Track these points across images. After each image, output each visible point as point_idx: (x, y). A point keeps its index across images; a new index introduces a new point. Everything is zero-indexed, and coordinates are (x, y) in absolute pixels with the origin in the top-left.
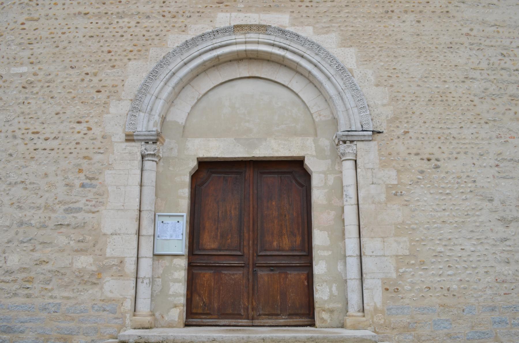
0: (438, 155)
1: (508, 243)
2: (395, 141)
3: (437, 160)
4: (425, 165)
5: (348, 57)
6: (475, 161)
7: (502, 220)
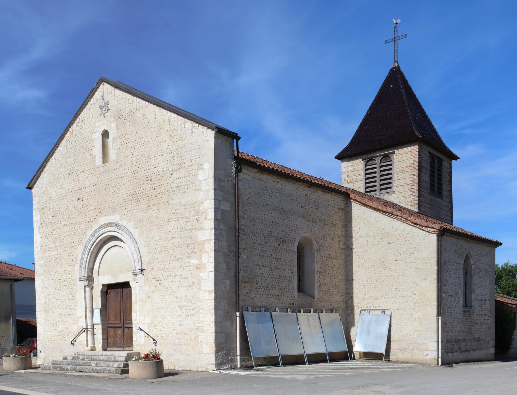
0: (161, 278)
1: (181, 317)
2: (150, 272)
3: (161, 281)
4: (157, 283)
6: (173, 280)
7: (180, 306)
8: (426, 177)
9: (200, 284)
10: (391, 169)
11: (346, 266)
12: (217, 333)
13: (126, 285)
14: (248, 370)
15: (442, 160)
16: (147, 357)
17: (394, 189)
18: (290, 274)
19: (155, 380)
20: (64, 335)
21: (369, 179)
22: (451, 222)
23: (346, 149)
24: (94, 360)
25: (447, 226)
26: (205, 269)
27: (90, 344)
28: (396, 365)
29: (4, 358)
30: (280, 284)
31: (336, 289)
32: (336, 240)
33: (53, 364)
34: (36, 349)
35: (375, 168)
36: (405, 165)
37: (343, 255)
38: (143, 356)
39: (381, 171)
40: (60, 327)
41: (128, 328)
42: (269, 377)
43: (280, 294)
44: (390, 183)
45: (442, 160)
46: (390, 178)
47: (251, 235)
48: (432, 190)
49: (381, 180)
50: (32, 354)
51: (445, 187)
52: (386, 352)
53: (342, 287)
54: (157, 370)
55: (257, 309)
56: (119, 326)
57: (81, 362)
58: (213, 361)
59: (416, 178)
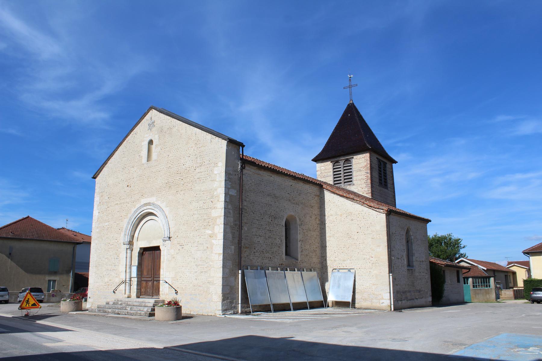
0: (184, 244)
4: (180, 248)
5: (167, 210)
7: (196, 265)
8: (376, 175)
9: (212, 248)
10: (351, 169)
11: (321, 236)
12: (224, 286)
13: (157, 248)
14: (247, 315)
15: (386, 163)
16: (169, 303)
17: (354, 182)
18: (280, 242)
19: (175, 322)
20: (108, 285)
21: (336, 175)
22: (395, 205)
23: (319, 154)
24: (129, 305)
25: (392, 208)
26: (217, 237)
27: (128, 293)
28: (360, 311)
29: (62, 302)
30: (272, 250)
31: (314, 254)
32: (314, 217)
33: (98, 307)
34: (87, 296)
35: (340, 168)
36: (361, 166)
37: (319, 228)
38: (167, 303)
39: (344, 170)
40: (106, 279)
41: (157, 281)
42: (263, 321)
43: (272, 257)
44: (351, 178)
45: (386, 163)
46: (351, 175)
47: (251, 213)
48: (380, 183)
49: (345, 176)
50: (84, 300)
51: (389, 181)
52: (352, 301)
53: (318, 252)
54: (177, 314)
55: (255, 268)
56: (150, 279)
57: (119, 306)
58: (220, 307)
59: (369, 176)
